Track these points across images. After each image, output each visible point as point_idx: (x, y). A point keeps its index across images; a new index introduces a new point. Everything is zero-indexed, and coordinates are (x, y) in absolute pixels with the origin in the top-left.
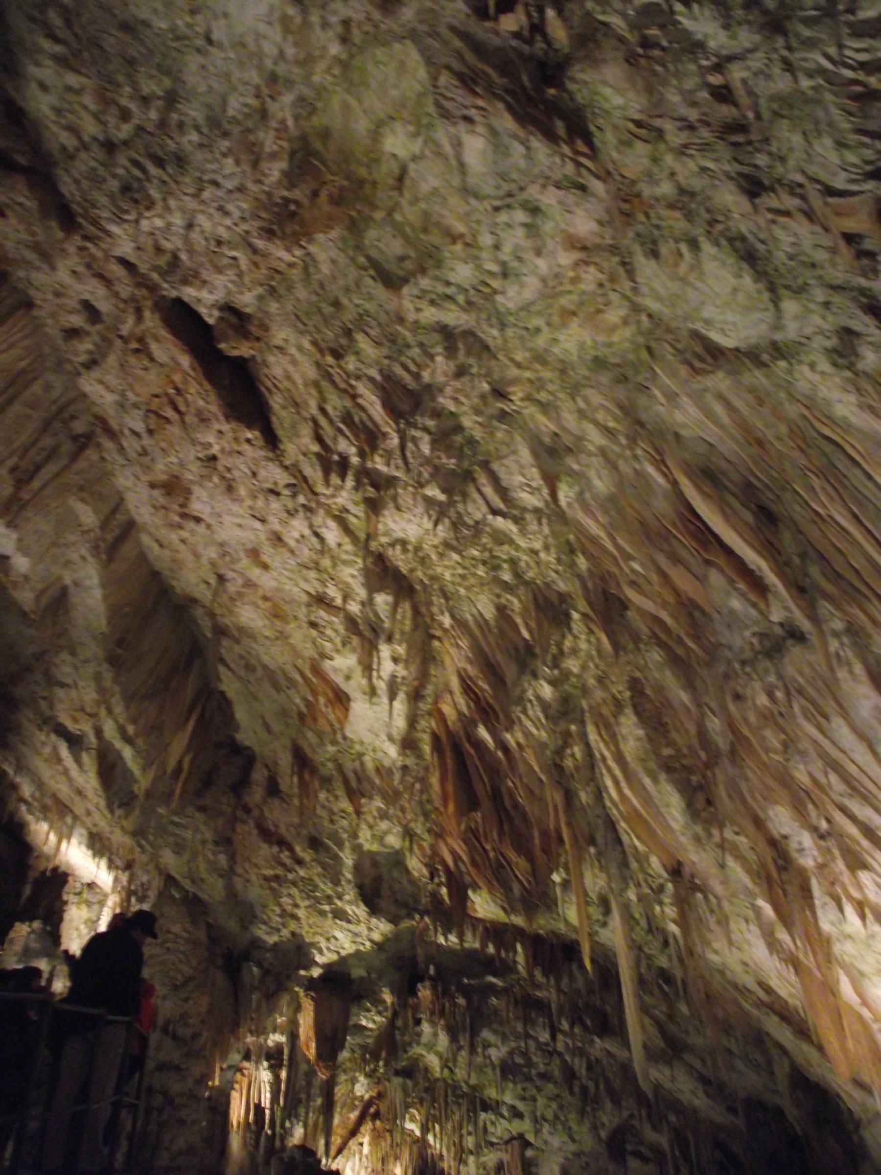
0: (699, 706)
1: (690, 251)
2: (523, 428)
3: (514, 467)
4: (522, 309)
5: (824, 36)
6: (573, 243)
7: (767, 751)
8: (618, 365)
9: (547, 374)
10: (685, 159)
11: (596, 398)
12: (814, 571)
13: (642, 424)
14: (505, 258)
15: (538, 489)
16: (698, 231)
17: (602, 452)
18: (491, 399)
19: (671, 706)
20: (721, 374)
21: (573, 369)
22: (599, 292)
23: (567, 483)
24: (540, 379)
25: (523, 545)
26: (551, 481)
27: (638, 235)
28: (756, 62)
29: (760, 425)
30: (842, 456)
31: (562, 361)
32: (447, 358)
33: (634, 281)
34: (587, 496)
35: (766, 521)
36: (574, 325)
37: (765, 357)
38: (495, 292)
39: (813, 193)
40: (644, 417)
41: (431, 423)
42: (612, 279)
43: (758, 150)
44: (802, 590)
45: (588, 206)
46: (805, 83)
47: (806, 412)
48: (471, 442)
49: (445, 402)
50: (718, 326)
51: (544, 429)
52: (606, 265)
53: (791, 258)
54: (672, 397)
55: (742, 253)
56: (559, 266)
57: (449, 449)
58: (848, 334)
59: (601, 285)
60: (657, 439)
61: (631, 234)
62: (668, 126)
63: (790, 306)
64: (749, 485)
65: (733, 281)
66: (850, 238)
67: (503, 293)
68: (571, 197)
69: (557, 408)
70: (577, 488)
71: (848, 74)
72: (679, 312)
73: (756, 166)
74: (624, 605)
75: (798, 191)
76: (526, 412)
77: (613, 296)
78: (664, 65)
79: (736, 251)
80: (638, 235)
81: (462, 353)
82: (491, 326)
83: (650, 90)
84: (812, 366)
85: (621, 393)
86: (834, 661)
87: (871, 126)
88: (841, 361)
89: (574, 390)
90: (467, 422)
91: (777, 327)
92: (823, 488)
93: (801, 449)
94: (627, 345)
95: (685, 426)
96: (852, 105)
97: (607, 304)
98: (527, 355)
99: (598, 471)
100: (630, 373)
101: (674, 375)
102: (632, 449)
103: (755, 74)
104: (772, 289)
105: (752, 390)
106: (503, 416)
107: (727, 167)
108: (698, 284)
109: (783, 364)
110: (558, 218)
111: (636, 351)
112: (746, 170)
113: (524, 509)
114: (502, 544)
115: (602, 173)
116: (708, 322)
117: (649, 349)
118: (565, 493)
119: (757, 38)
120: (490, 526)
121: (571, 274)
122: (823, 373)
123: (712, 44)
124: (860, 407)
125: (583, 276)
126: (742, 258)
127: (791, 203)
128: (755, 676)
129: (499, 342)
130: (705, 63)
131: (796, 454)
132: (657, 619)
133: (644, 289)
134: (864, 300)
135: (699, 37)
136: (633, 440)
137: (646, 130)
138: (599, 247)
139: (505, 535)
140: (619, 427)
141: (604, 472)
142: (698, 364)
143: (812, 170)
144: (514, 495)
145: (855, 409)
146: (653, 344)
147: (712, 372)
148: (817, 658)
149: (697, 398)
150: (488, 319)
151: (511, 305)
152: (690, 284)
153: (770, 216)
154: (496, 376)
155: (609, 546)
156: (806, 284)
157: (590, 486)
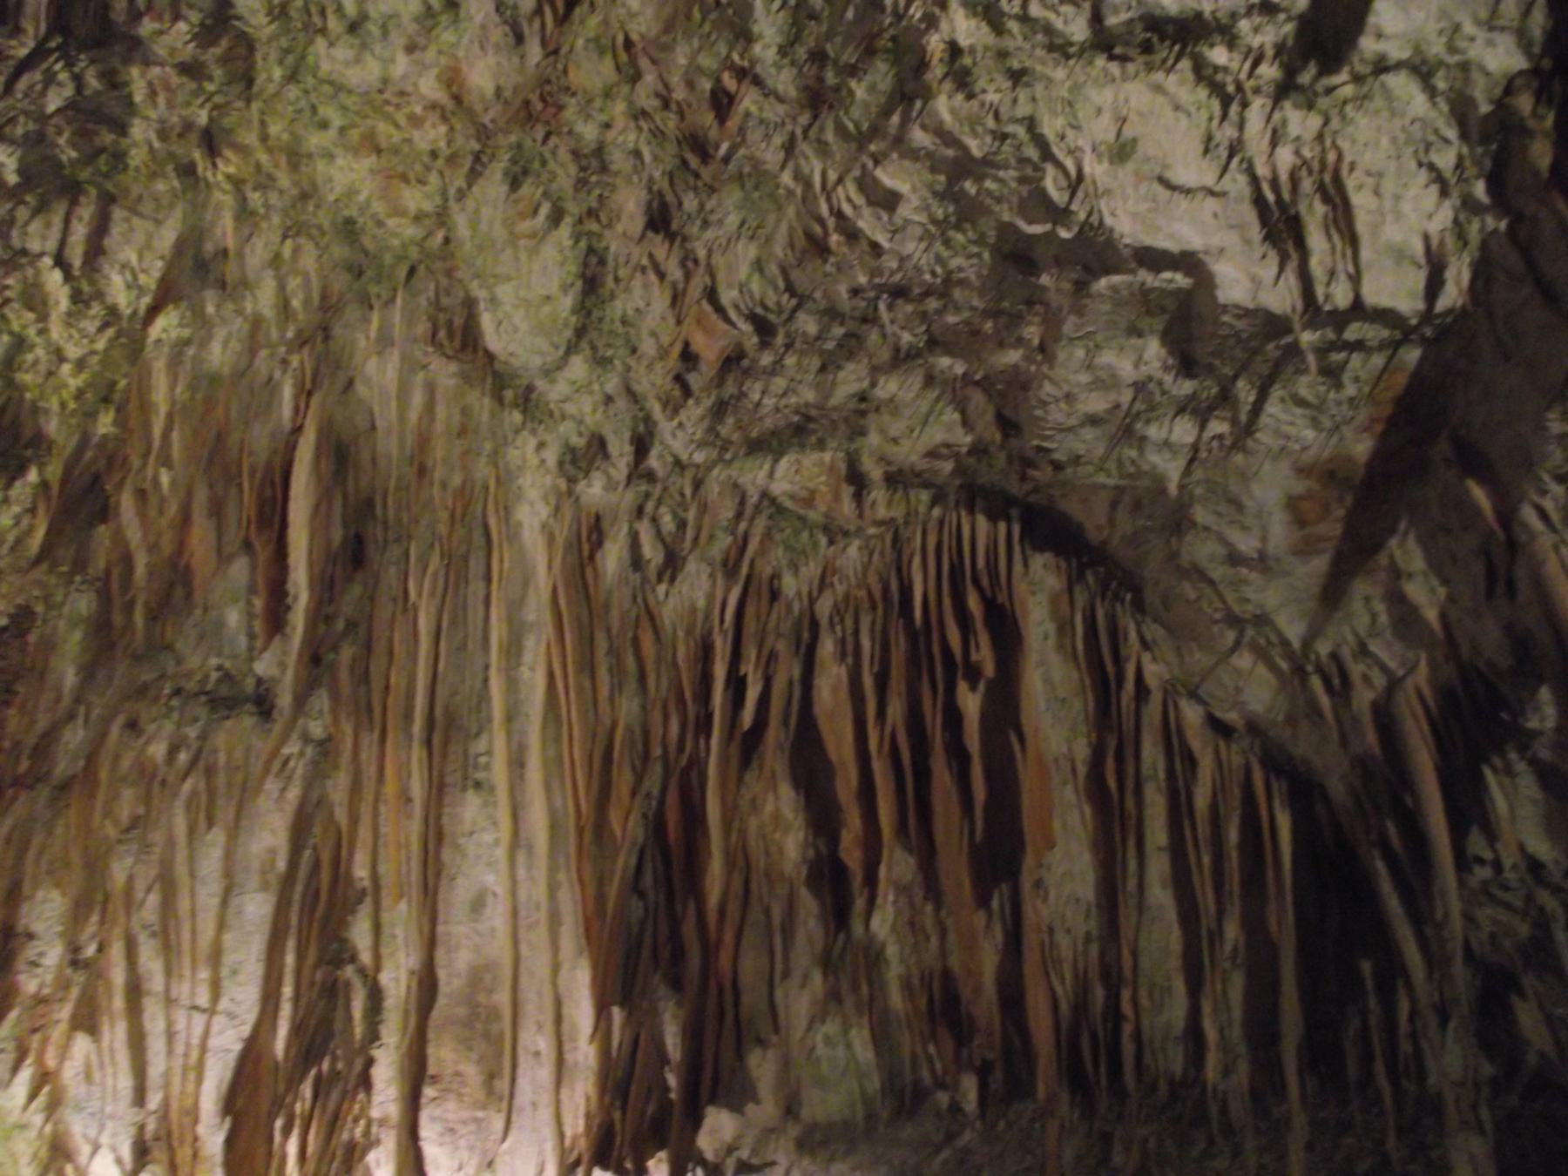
0: (78, 700)
1: (548, 218)
2: (197, 208)
3: (140, 237)
4: (331, 83)
5: (838, 157)
6: (453, 80)
7: (107, 814)
8: (366, 253)
9: (284, 180)
10: (632, 125)
11: (308, 261)
12: (347, 653)
13: (327, 338)
14: (373, 14)
15: (141, 291)
16: (573, 209)
17: (257, 322)
18: (194, 137)
19: (42, 675)
20: (453, 367)
21: (317, 207)
22: (426, 159)
23: (182, 317)
24: (271, 178)
25: (55, 335)
26: (165, 296)
27: (519, 146)
28: (775, 111)
29: (439, 453)
30: (482, 561)
31: (314, 184)
32: (195, 37)
33: (470, 186)
34: (191, 352)
35: (351, 556)
36: (370, 161)
37: (509, 394)
38: (323, 31)
39: (699, 281)
40: (337, 331)
41: (93, 82)
42: (452, 160)
43: (695, 188)
44: (316, 660)
45: (505, 63)
46: (786, 178)
47: (492, 484)
48: (119, 158)
49: (138, 81)
50: (500, 315)
51: (218, 232)
52: (459, 141)
53: (624, 322)
54: (384, 341)
55: (589, 273)
56: (415, 85)
57: (82, 136)
58: (598, 445)
59: (434, 154)
60: (327, 367)
61: (513, 138)
62: (649, 78)
63: (578, 367)
64: (370, 503)
65: (554, 288)
66: (689, 357)
67: (331, 45)
68: (498, 34)
69: (256, 225)
70: (186, 333)
71: (824, 209)
72: (479, 262)
73: (680, 204)
74: (105, 512)
75: (690, 264)
76: (217, 195)
77: (434, 180)
78: (704, 19)
79: (585, 265)
80: (519, 146)
81: (217, 51)
82: (281, 62)
83: (669, 27)
84: (541, 446)
85: (340, 282)
86: (276, 765)
87: (795, 275)
88: (568, 466)
89: (292, 230)
90: (139, 131)
91: (549, 373)
92: (435, 574)
93: (453, 516)
94: (396, 242)
95: (368, 382)
96: (801, 242)
97: (422, 182)
98: (285, 136)
99: (230, 334)
100: (369, 273)
101: (410, 321)
102: (290, 351)
103: (761, 121)
104: (580, 332)
105: (465, 412)
106: (188, 171)
107: (657, 174)
108: (523, 257)
109: (517, 417)
110: (465, 40)
111: (400, 259)
112: (670, 197)
113: (99, 295)
114: (31, 309)
115: (551, 48)
116: (493, 300)
117: (412, 271)
118: (167, 325)
119: (793, 93)
120: (38, 273)
121: (418, 110)
122: (543, 461)
123: (757, 49)
124: (544, 526)
125: (427, 125)
126: (583, 276)
127: (675, 273)
128: (175, 716)
129: (271, 88)
130: (736, 57)
131: (444, 515)
132: (127, 560)
133: (470, 203)
134: (641, 428)
135: (756, 29)
136: (302, 341)
137: (628, 57)
138: (471, 114)
139: (45, 303)
140: (301, 317)
141: (235, 345)
142: (442, 334)
143: (718, 260)
144: (106, 268)
145: (536, 523)
146: (421, 269)
147: (448, 357)
148: (262, 746)
149: (410, 366)
150: (287, 51)
151: (325, 67)
152: (516, 248)
153: (645, 261)
154: (227, 122)
155: (157, 431)
156: (610, 360)
157: (204, 343)
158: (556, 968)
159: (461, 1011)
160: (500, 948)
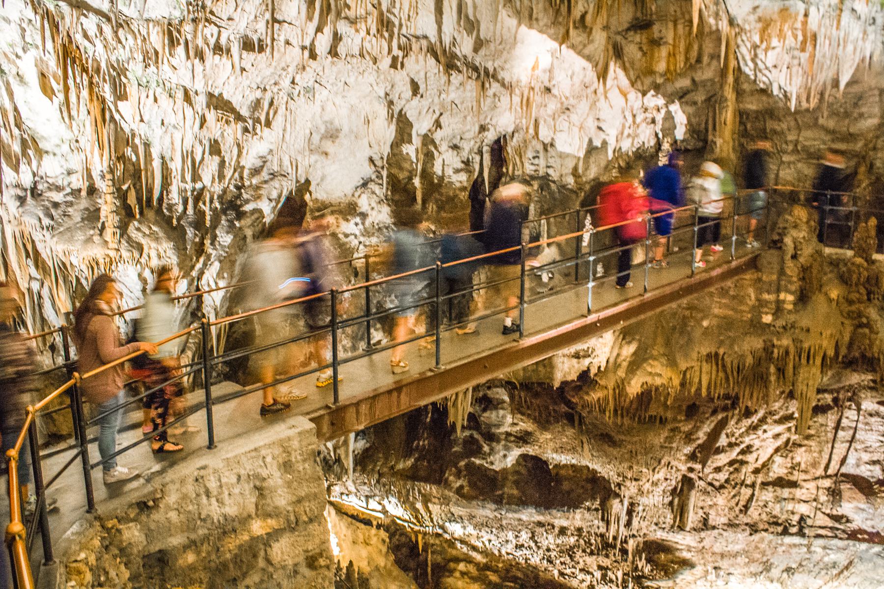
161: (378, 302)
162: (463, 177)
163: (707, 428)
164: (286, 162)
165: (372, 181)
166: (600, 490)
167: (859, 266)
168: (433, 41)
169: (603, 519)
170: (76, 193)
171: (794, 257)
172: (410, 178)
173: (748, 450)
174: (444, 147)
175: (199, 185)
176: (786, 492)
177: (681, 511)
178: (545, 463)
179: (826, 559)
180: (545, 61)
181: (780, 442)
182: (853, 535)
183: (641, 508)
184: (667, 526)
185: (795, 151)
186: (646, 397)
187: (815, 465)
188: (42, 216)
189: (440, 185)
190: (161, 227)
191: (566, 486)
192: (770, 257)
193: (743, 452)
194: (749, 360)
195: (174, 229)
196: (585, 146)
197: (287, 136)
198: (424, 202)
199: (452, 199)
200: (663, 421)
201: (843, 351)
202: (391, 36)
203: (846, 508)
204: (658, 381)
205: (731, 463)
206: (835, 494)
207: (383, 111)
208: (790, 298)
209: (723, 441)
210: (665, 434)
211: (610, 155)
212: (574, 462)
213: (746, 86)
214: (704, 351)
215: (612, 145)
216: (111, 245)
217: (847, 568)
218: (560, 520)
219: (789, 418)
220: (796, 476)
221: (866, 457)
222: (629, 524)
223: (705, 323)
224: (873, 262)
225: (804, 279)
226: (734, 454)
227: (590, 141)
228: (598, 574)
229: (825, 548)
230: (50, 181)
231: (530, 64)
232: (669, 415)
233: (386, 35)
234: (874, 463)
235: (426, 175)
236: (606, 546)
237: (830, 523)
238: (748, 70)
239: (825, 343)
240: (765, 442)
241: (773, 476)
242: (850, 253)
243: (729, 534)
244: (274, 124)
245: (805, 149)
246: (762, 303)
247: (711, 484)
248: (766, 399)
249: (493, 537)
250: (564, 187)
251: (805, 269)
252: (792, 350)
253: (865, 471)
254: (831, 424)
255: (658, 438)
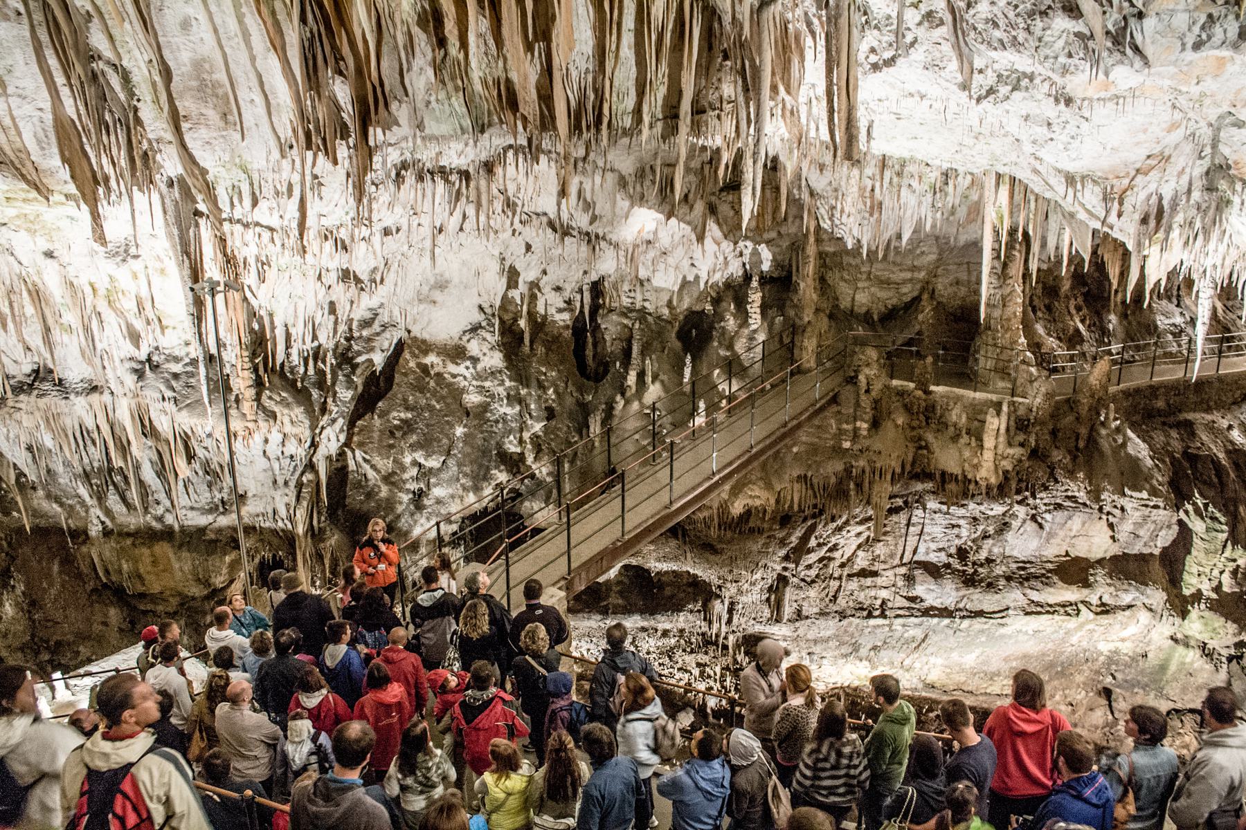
158: (253, 59)
159: (194, 84)
160: (208, 46)
161: (497, 443)
162: (566, 316)
163: (799, 533)
164: (396, 312)
165: (481, 327)
166: (702, 593)
167: (919, 399)
168: (552, 217)
169: (705, 619)
170: (194, 362)
171: (867, 391)
172: (515, 320)
173: (834, 548)
174: (547, 289)
175: (316, 344)
176: (869, 581)
177: (778, 606)
178: (648, 571)
179: (906, 635)
180: (650, 226)
181: (861, 540)
182: (927, 612)
183: (740, 606)
184: (764, 619)
185: (869, 278)
186: (748, 514)
187: (892, 556)
188: (163, 388)
189: (543, 324)
190: (287, 391)
191: (668, 591)
192: (847, 393)
193: (830, 550)
194: (833, 480)
195: (299, 391)
196: (679, 281)
197: (398, 290)
198: (532, 342)
199: (557, 339)
200: (760, 531)
201: (908, 468)
202: (514, 215)
203: (919, 590)
204: (758, 502)
205: (821, 560)
206: (910, 579)
207: (496, 267)
208: (865, 426)
209: (813, 542)
210: (761, 541)
211: (702, 286)
212: (675, 568)
213: (825, 237)
214: (795, 473)
215: (704, 277)
216: (249, 417)
217: (923, 641)
218: (662, 622)
219: (869, 519)
220: (877, 567)
221: (933, 546)
222: (729, 622)
223: (795, 450)
224: (930, 393)
225: (875, 408)
226: (822, 552)
227: (684, 277)
228: (696, 672)
229: (904, 626)
230: (167, 352)
231: (636, 230)
232: (766, 526)
233: (510, 214)
234: (940, 550)
235: (531, 315)
236: (708, 642)
237: (907, 604)
238: (826, 225)
239: (893, 464)
240: (848, 541)
241: (856, 568)
242: (912, 385)
243: (822, 622)
244: (386, 281)
245: (876, 277)
246: (841, 432)
247: (803, 580)
248: (848, 507)
249: (592, 646)
250: (659, 317)
251: (876, 402)
252: (868, 469)
253: (933, 558)
254: (904, 522)
255: (755, 546)
